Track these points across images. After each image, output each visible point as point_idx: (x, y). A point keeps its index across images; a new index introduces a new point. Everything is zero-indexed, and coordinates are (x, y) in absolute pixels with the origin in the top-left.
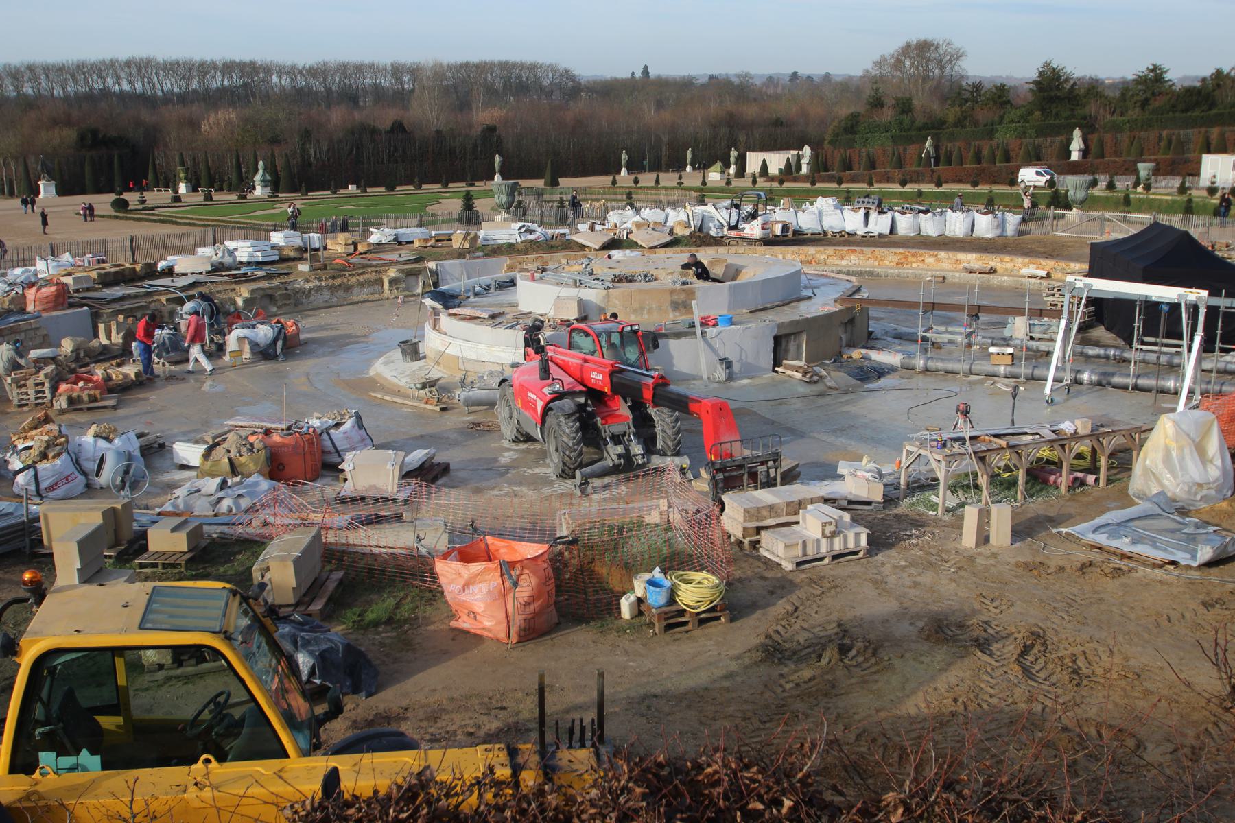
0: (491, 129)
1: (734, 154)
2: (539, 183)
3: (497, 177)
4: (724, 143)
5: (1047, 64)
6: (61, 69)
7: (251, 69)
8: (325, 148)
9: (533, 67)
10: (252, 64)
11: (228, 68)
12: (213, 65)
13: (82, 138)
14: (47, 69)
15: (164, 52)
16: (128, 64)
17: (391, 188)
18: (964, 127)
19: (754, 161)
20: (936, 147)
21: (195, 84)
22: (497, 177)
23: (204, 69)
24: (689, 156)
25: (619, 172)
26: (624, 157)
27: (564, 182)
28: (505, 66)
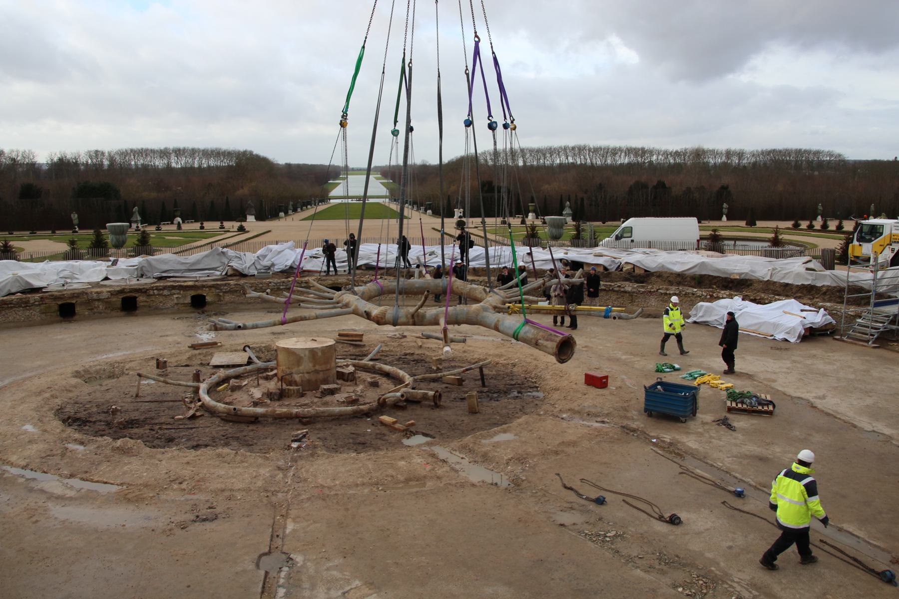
0: (724, 188)
6: (539, 151)
7: (643, 152)
9: (817, 153)
10: (643, 149)
11: (629, 151)
12: (620, 150)
13: (483, 185)
14: (531, 151)
15: (593, 143)
16: (573, 148)
21: (609, 162)
23: (615, 152)
25: (815, 219)
26: (820, 207)
28: (799, 152)
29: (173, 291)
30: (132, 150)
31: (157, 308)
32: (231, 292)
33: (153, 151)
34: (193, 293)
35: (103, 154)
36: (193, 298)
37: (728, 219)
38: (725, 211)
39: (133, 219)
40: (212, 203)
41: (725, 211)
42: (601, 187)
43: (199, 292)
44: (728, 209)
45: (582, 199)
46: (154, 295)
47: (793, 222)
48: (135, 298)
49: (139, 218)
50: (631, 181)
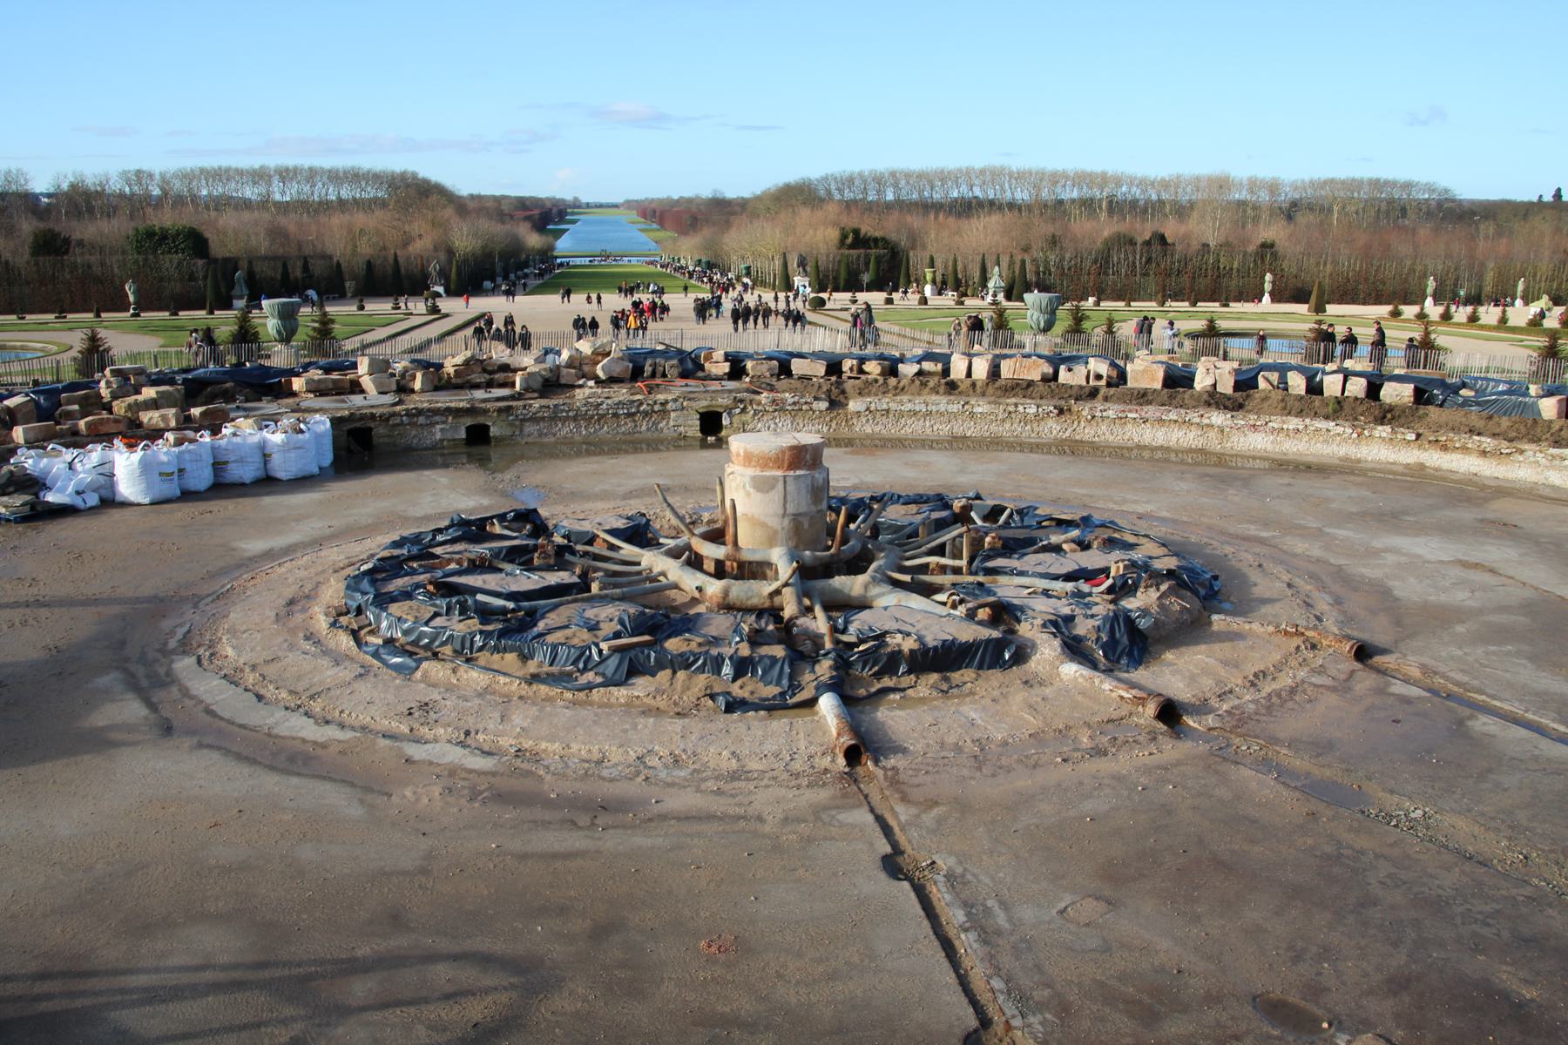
0: (1267, 246)
3: (1266, 298)
8: (1068, 256)
9: (1408, 186)
10: (1104, 176)
11: (1081, 178)
12: (1065, 175)
13: (844, 237)
14: (908, 175)
16: (983, 172)
22: (1266, 298)
23: (1055, 178)
24: (1520, 287)
29: (437, 418)
30: (202, 170)
31: (409, 449)
32: (534, 419)
33: (240, 172)
34: (469, 421)
35: (151, 176)
36: (469, 429)
37: (1273, 301)
38: (1268, 287)
39: (236, 292)
40: (369, 263)
41: (1268, 287)
42: (1054, 241)
43: (481, 420)
44: (1273, 283)
45: (1023, 262)
46: (402, 423)
47: (1389, 308)
48: (371, 429)
49: (246, 292)
50: (1107, 228)
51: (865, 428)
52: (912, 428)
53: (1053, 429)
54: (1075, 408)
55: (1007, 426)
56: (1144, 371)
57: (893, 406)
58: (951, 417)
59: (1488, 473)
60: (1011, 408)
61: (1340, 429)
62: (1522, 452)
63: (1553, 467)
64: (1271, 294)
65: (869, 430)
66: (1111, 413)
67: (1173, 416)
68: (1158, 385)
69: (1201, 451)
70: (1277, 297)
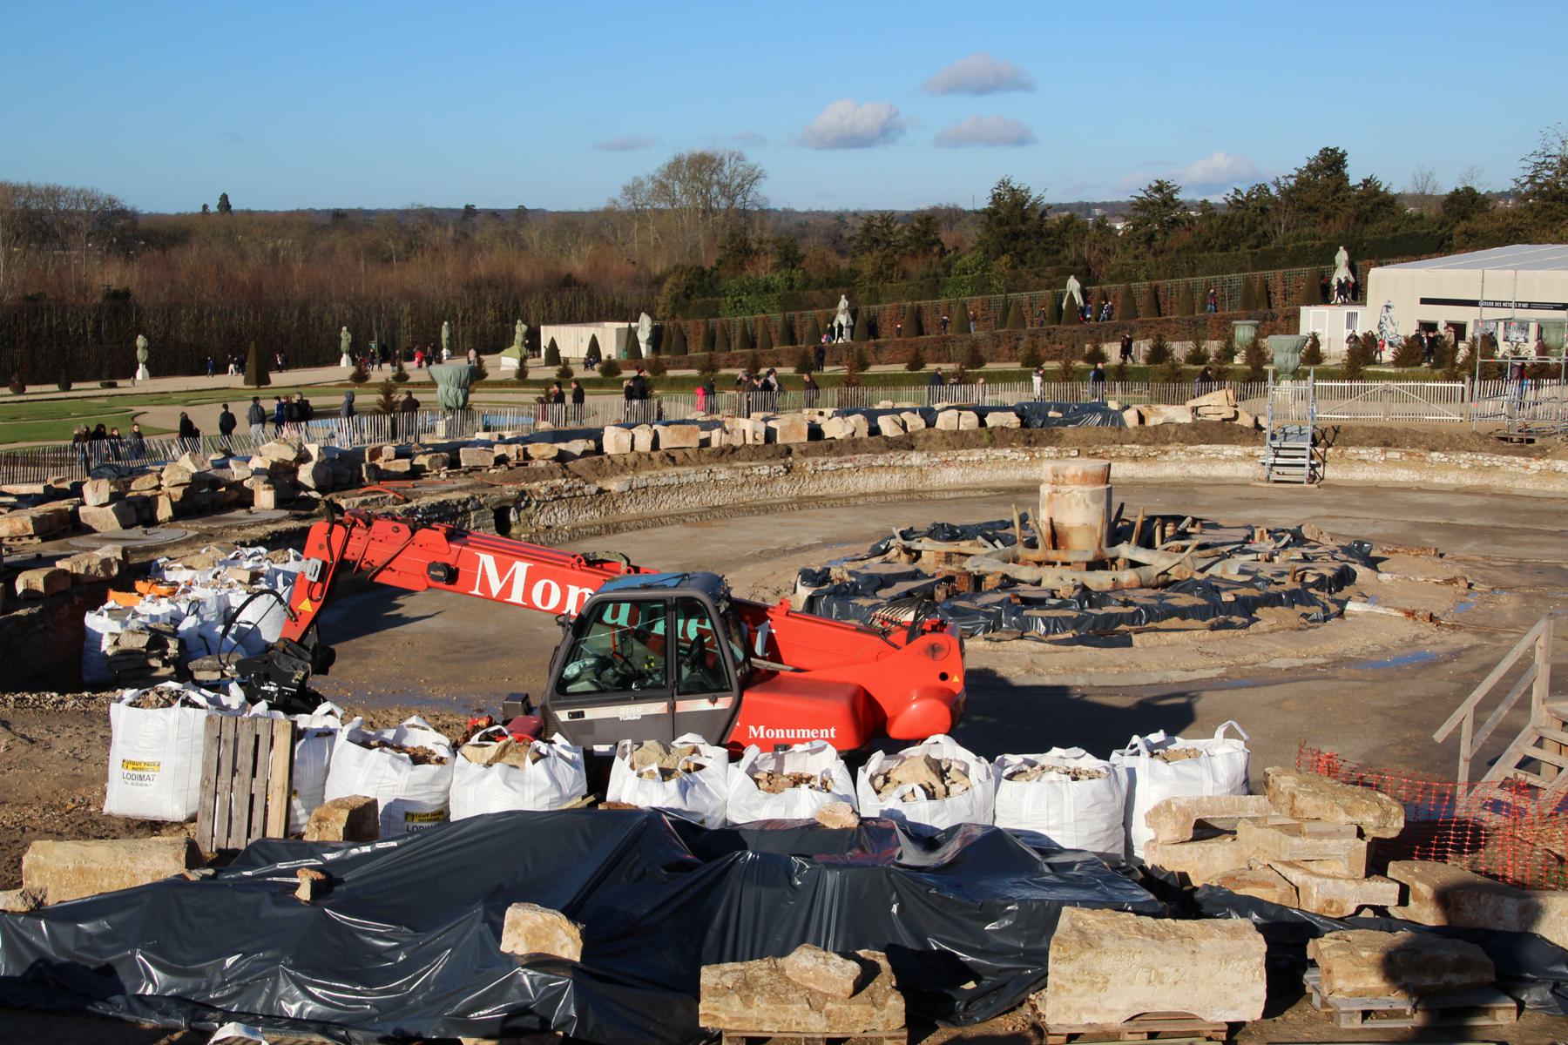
1: (520, 328)
2: (233, 379)
4: (490, 314)
5: (1003, 184)
17: (66, 387)
18: (889, 279)
19: (571, 340)
20: (854, 313)
22: (141, 373)
24: (445, 334)
26: (345, 337)
27: (277, 378)
38: (141, 355)
51: (630, 510)
52: (670, 503)
53: (784, 489)
54: (797, 464)
55: (746, 490)
56: (791, 426)
57: (651, 482)
58: (701, 486)
59: (1141, 475)
60: (748, 472)
61: (1015, 455)
62: (1166, 453)
63: (1192, 462)
64: (148, 365)
65: (632, 510)
66: (830, 466)
67: (880, 461)
68: (805, 439)
69: (910, 491)
70: (155, 371)
